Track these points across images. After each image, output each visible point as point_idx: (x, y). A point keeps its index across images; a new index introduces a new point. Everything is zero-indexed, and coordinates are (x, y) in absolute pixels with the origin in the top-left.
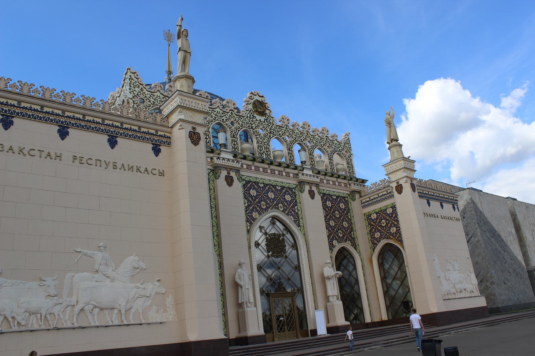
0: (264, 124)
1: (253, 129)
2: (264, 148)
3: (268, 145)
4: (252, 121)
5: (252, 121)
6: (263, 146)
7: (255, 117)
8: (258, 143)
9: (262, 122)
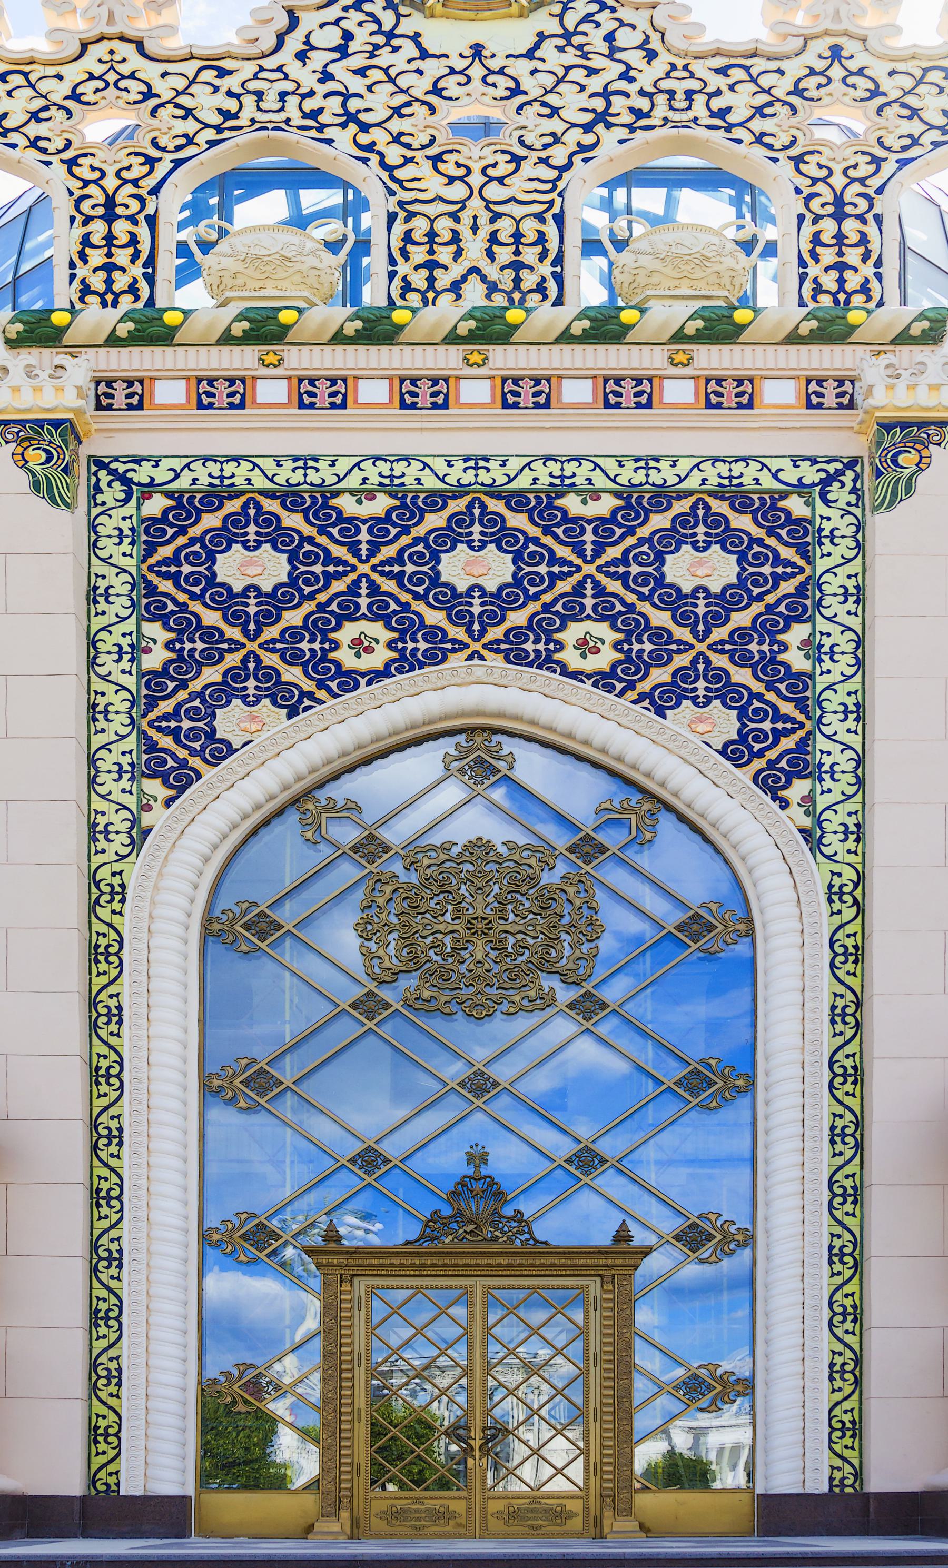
0: (521, 68)
1: (365, 128)
2: (474, 248)
3: (540, 217)
4: (361, 72)
5: (361, 72)
6: (475, 228)
7: (415, 38)
8: (411, 215)
9: (494, 64)
